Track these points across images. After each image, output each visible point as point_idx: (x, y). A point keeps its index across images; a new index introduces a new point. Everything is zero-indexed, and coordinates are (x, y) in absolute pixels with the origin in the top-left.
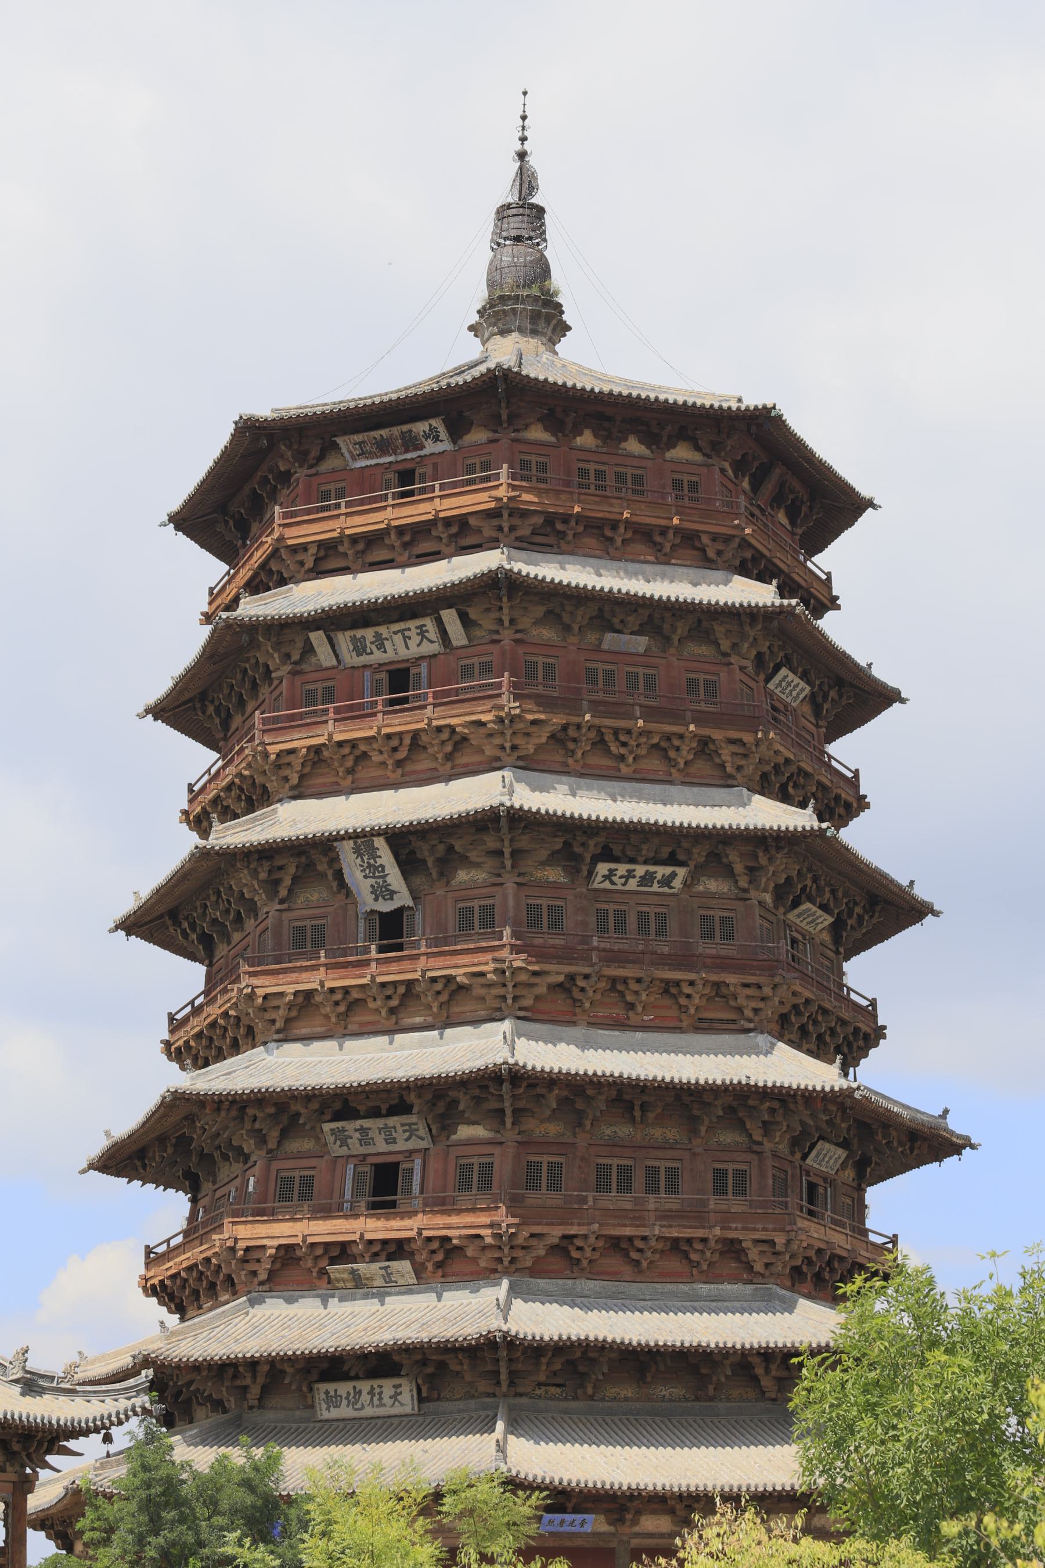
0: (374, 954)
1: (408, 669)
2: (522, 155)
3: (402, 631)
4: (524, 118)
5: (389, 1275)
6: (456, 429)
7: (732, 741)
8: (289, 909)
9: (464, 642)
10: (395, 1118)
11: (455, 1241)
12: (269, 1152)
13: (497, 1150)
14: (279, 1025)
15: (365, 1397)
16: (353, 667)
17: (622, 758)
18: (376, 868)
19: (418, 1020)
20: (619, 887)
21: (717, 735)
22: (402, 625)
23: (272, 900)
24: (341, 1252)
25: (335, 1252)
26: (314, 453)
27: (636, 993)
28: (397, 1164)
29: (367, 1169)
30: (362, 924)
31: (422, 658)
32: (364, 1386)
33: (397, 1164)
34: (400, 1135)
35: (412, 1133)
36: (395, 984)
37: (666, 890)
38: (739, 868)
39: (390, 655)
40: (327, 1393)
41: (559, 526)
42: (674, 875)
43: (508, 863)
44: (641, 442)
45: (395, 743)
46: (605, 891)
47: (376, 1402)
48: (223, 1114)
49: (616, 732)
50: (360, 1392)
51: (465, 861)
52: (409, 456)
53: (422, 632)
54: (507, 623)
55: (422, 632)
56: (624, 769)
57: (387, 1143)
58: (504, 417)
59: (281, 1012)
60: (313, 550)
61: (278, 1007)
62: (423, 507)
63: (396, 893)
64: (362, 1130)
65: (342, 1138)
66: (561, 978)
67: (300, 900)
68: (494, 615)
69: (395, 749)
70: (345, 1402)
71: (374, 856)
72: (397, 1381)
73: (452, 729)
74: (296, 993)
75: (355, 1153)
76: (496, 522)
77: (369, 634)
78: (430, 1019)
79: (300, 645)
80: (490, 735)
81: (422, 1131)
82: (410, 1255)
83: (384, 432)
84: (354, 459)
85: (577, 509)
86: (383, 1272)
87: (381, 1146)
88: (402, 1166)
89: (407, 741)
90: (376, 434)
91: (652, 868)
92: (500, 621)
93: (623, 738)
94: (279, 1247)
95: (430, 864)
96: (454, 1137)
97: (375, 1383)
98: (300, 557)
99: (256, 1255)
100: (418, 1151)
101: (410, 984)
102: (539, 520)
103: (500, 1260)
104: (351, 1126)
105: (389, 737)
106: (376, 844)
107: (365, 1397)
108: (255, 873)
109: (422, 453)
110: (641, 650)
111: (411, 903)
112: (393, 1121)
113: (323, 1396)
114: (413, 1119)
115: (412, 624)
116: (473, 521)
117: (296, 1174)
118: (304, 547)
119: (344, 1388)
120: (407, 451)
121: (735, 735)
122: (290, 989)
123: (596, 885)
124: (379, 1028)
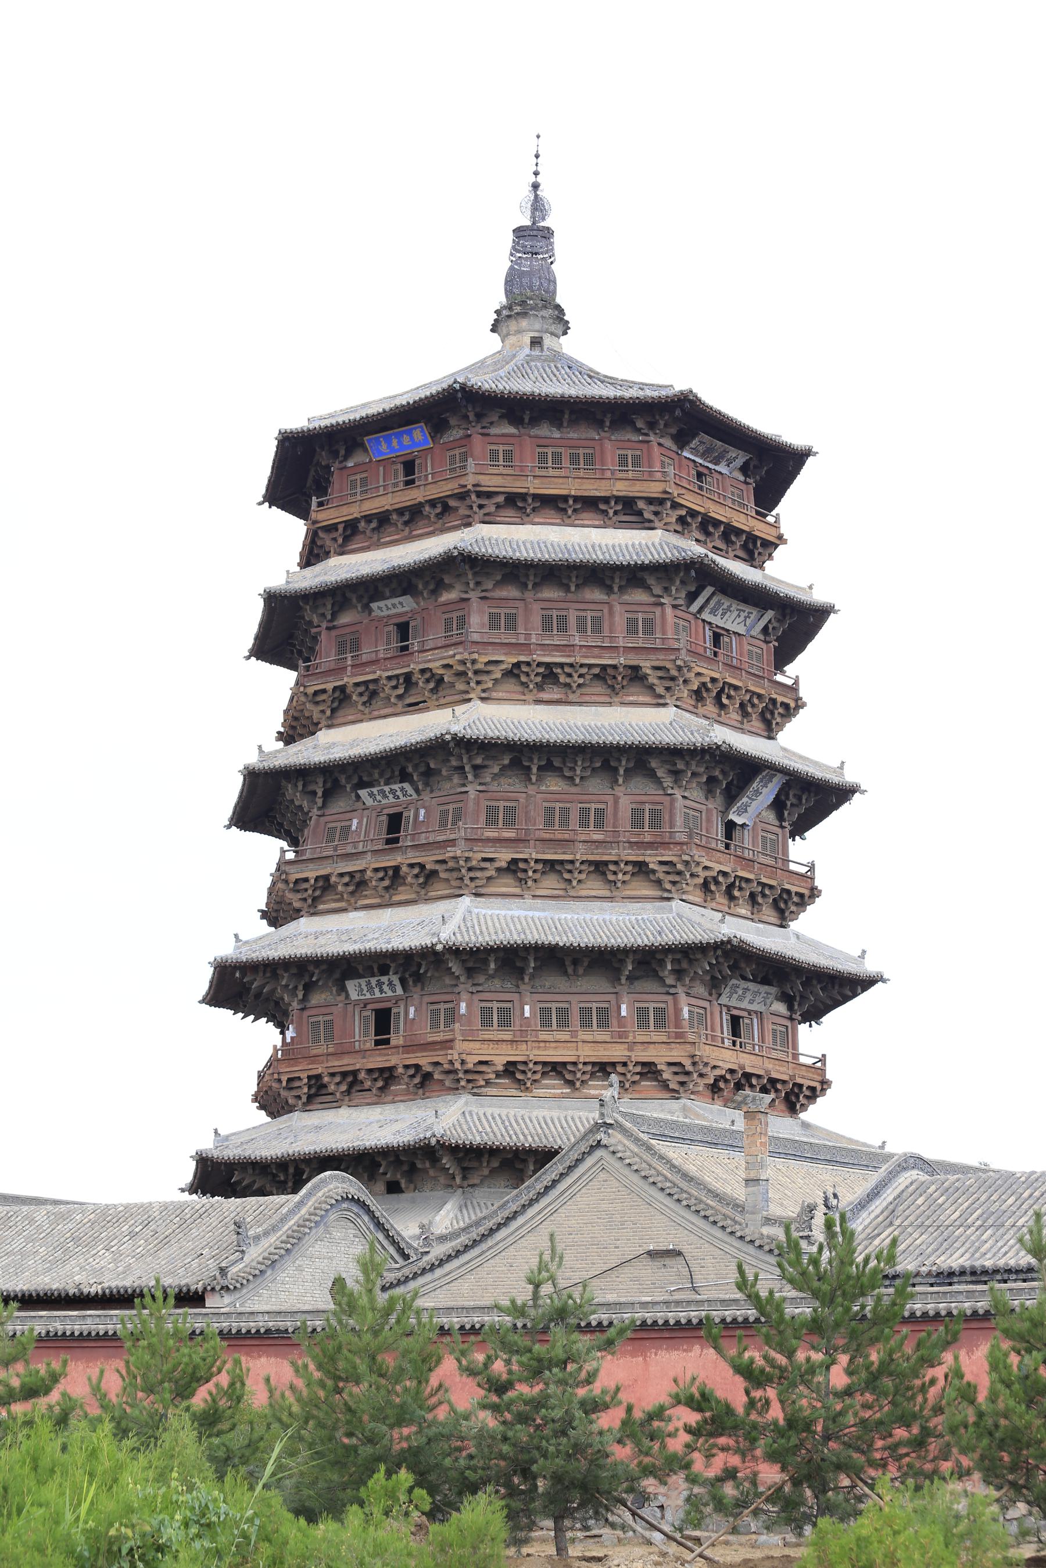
10: (766, 987)
16: (703, 621)
52: (710, 466)
63: (746, 811)
77: (726, 602)
87: (745, 1005)
109: (717, 468)
114: (773, 990)
115: (748, 609)
118: (675, 506)
122: (718, 867)
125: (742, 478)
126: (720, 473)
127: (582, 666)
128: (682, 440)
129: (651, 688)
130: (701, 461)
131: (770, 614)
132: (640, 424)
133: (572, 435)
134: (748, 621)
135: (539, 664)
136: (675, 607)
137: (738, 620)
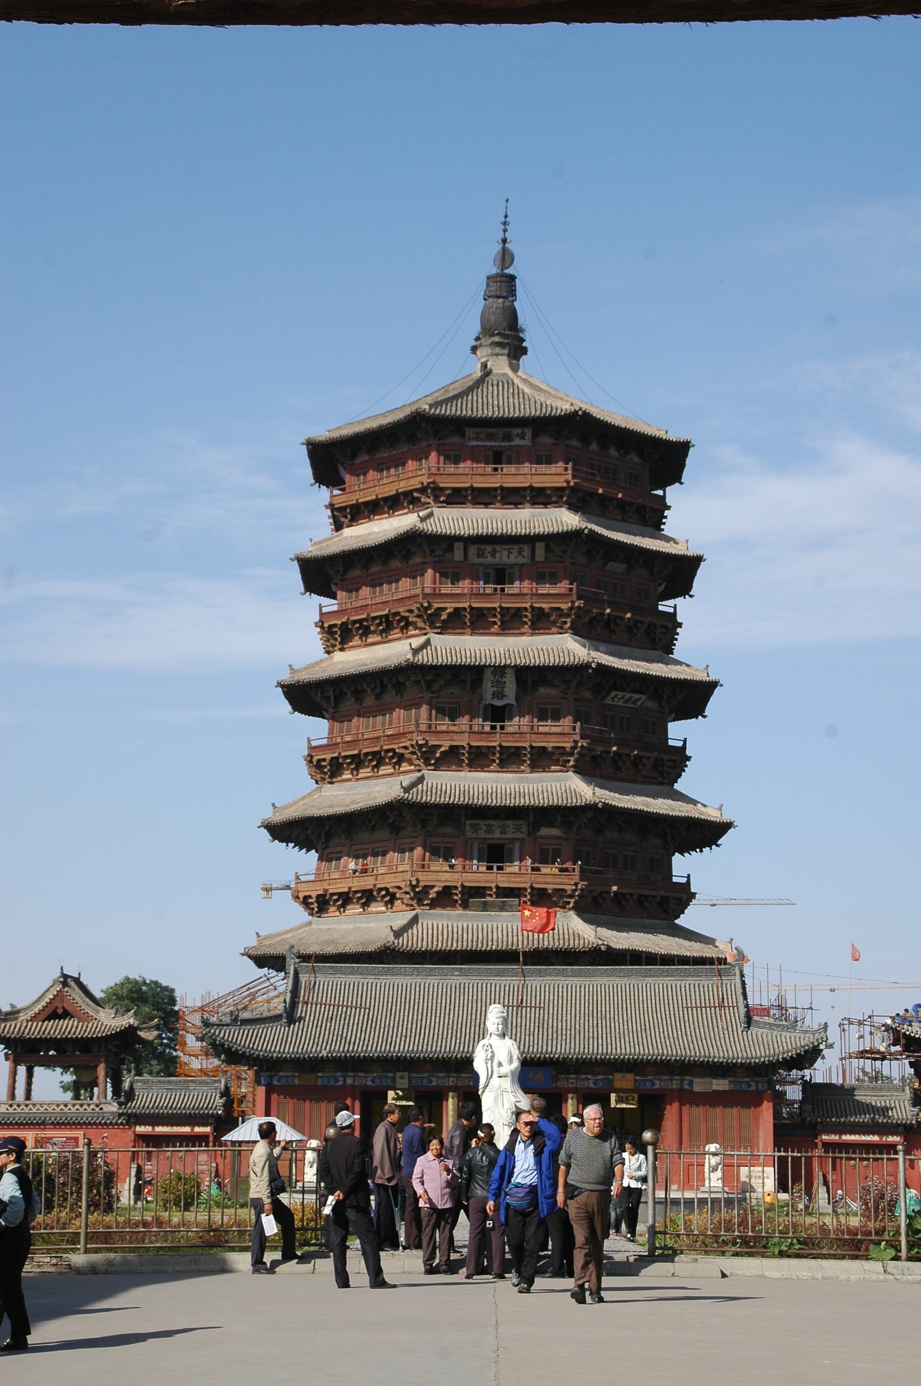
0: (498, 729)
1: (505, 569)
2: (504, 241)
3: (509, 549)
4: (506, 216)
5: (504, 906)
6: (535, 435)
7: (661, 626)
8: (438, 697)
9: (542, 559)
12: (427, 832)
17: (613, 631)
18: (501, 683)
21: (658, 623)
23: (427, 691)
24: (479, 892)
27: (624, 762)
29: (485, 846)
31: (516, 564)
35: (518, 829)
36: (507, 747)
38: (665, 696)
41: (588, 499)
44: (617, 450)
45: (505, 612)
49: (616, 617)
51: (551, 685)
52: (503, 444)
53: (520, 552)
55: (520, 552)
56: (614, 638)
57: (501, 833)
62: (520, 478)
64: (489, 826)
65: (475, 828)
73: (541, 609)
74: (452, 747)
77: (489, 548)
81: (524, 829)
82: (518, 896)
83: (494, 431)
84: (469, 440)
85: (600, 491)
87: (497, 834)
88: (507, 846)
89: (512, 612)
90: (490, 430)
91: (632, 695)
92: (565, 551)
93: (618, 621)
95: (530, 682)
96: (539, 833)
98: (437, 493)
101: (519, 747)
102: (581, 495)
104: (481, 823)
109: (512, 444)
110: (621, 571)
111: (513, 702)
114: (521, 822)
115: (516, 547)
117: (442, 845)
120: (502, 441)
121: (665, 623)
123: (606, 702)
126: (518, 446)
127: (375, 618)
128: (462, 435)
129: (414, 624)
130: (493, 444)
132: (419, 436)
133: (395, 452)
134: (525, 554)
135: (355, 622)
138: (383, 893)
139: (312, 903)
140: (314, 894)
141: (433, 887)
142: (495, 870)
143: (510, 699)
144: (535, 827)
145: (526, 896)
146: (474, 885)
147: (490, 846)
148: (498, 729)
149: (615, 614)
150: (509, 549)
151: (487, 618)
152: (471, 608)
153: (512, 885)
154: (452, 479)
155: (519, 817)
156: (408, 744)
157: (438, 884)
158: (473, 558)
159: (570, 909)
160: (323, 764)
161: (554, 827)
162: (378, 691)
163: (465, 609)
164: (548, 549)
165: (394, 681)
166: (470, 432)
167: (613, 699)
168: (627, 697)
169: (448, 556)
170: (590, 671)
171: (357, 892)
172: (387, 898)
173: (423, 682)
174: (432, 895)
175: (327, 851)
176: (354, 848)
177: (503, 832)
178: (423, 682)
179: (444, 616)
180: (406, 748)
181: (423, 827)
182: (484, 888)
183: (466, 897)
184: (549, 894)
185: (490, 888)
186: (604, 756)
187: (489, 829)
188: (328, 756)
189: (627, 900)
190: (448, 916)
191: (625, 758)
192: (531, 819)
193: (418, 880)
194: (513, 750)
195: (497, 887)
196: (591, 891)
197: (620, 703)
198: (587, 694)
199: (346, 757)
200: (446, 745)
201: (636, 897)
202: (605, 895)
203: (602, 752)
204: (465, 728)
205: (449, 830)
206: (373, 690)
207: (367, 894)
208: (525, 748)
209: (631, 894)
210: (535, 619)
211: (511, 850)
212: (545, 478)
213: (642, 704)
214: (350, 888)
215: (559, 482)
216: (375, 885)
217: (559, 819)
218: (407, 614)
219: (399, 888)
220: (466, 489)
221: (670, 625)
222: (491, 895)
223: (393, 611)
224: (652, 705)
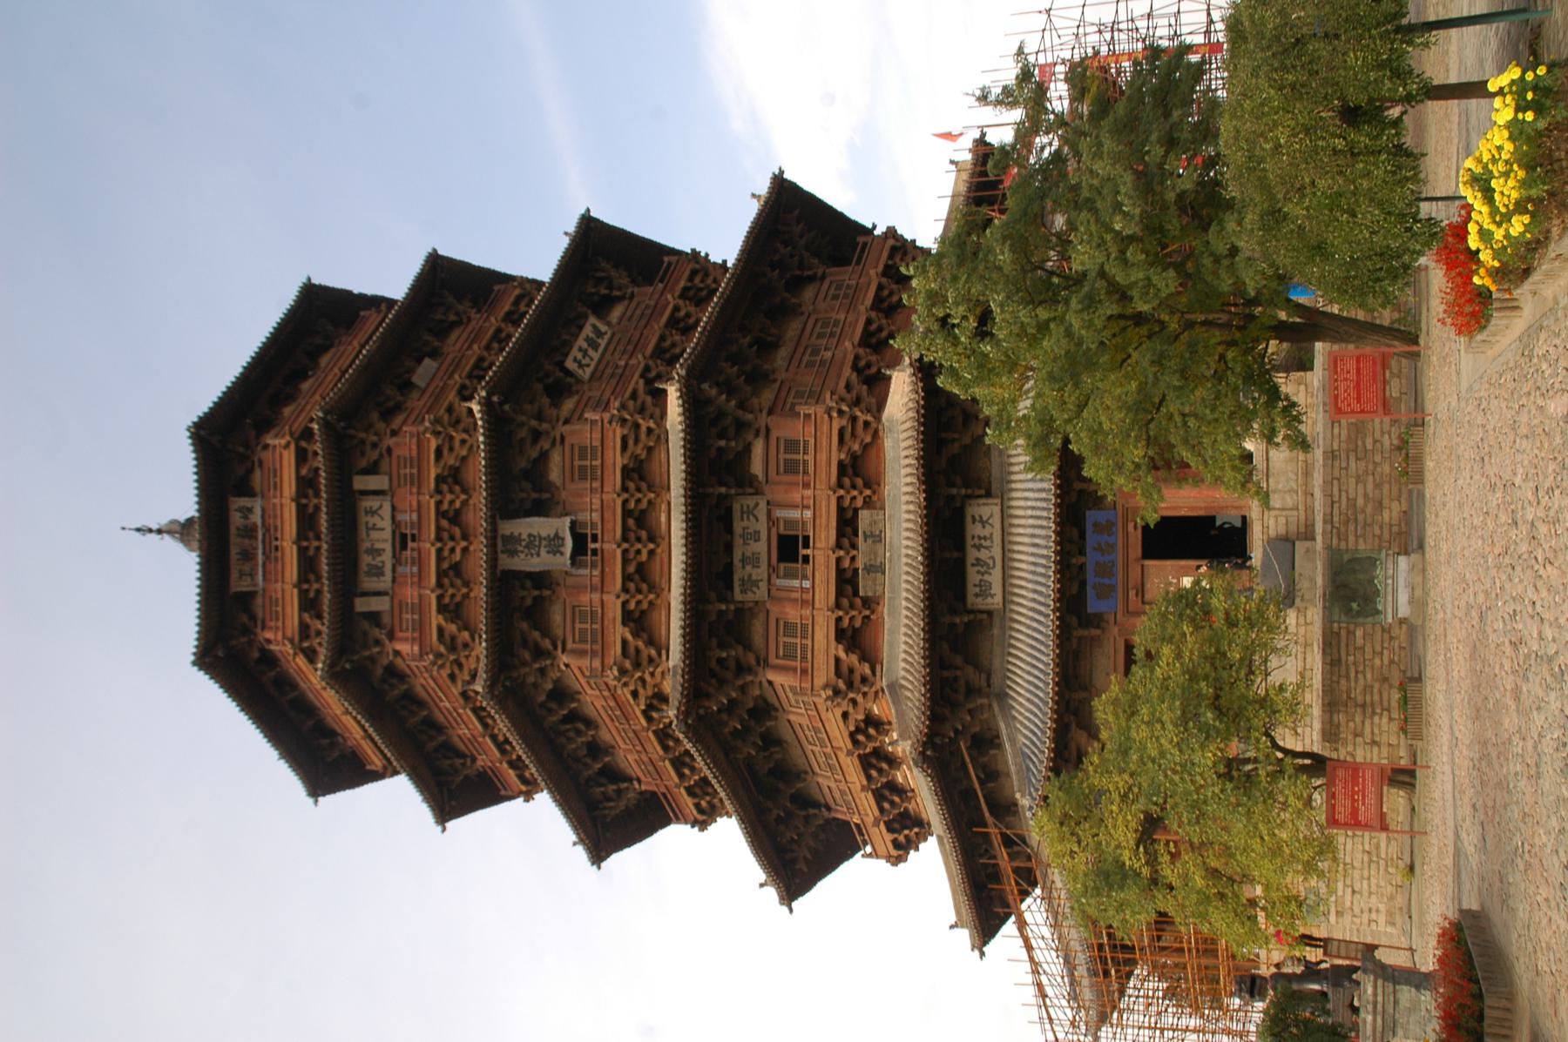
0: (597, 546)
2: (159, 531)
3: (368, 529)
4: (138, 530)
5: (872, 535)
6: (246, 490)
11: (843, 456)
12: (758, 664)
13: (774, 434)
14: (653, 652)
15: (983, 554)
16: (394, 581)
18: (531, 542)
19: (663, 518)
20: (593, 364)
21: (507, 308)
22: (363, 529)
23: (554, 658)
24: (846, 582)
25: (849, 589)
26: (245, 618)
28: (781, 538)
29: (782, 566)
30: (582, 572)
31: (393, 518)
32: (972, 554)
33: (781, 538)
34: (753, 526)
35: (750, 512)
36: (625, 529)
37: (607, 337)
38: (604, 291)
39: (388, 547)
40: (977, 595)
42: (594, 326)
43: (545, 426)
45: (445, 535)
46: (593, 373)
47: (987, 543)
48: (711, 690)
50: (978, 559)
52: (260, 537)
54: (375, 438)
55: (373, 512)
58: (241, 450)
59: (640, 644)
60: (306, 616)
61: (637, 650)
62: (287, 515)
63: (557, 535)
64: (744, 561)
66: (642, 382)
67: (559, 632)
68: (368, 447)
69: (452, 538)
70: (986, 577)
71: (518, 539)
72: (969, 519)
73: (440, 479)
74: (624, 624)
75: (765, 576)
76: (310, 455)
77: (366, 560)
78: (664, 507)
79: (365, 625)
80: (451, 449)
81: (750, 501)
82: (856, 511)
86: (870, 541)
87: (761, 547)
88: (782, 531)
89: (445, 523)
92: (375, 446)
94: (839, 639)
95: (534, 495)
96: (761, 477)
97: (969, 542)
98: (313, 633)
99: (845, 669)
100: (769, 513)
101: (626, 513)
103: (867, 424)
105: (439, 538)
106: (507, 533)
107: (983, 554)
108: (524, 664)
111: (567, 520)
112: (738, 527)
113: (979, 600)
114: (736, 507)
115: (364, 519)
116: (304, 472)
119: (973, 576)
120: (256, 538)
121: (512, 299)
123: (587, 376)
124: (665, 555)
125: (258, 473)
126: (263, 517)
130: (260, 552)
131: (360, 482)
132: (256, 654)
136: (391, 636)
137: (381, 524)
138: (861, 738)
139: (906, 837)
140: (889, 837)
141: (837, 660)
142: (809, 552)
143: (561, 526)
144: (747, 483)
145: (854, 498)
146: (833, 589)
147: (781, 559)
148: (597, 546)
149: (468, 368)
150: (368, 529)
151: (457, 563)
152: (440, 585)
153: (833, 523)
154: (288, 610)
155: (730, 510)
156: (627, 691)
157: (833, 652)
158: (385, 582)
159: (878, 419)
160: (704, 803)
161: (748, 449)
162: (582, 727)
163: (440, 598)
164: (373, 469)
165: (553, 705)
166: (238, 585)
167: (581, 366)
168: (585, 345)
169: (386, 620)
170: (495, 399)
171: (869, 778)
172: (872, 731)
173: (537, 666)
174: (854, 659)
175: (832, 805)
176: (817, 769)
177: (756, 536)
178: (537, 666)
179: (452, 628)
180: (635, 694)
181: (750, 670)
182: (840, 572)
183: (858, 602)
184: (854, 457)
185: (839, 560)
186: (653, 374)
187: (753, 560)
188: (689, 801)
189: (880, 329)
190: (892, 632)
191: (668, 343)
192: (723, 490)
193: (826, 687)
194: (631, 522)
195: (839, 546)
196: (848, 387)
197: (596, 355)
198: (569, 405)
199: (681, 776)
200: (619, 633)
201: (873, 314)
202: (862, 363)
203: (642, 376)
204: (596, 596)
205: (757, 628)
206: (579, 732)
207: (874, 761)
208: (625, 502)
209: (869, 322)
210: (457, 488)
211: (788, 523)
212: (286, 477)
213: (609, 324)
214: (863, 789)
215: (289, 458)
216: (849, 753)
217: (723, 443)
218: (459, 683)
219: (845, 715)
220: (303, 594)
221: (517, 292)
222: (853, 559)
223: (462, 701)
224: (616, 313)
